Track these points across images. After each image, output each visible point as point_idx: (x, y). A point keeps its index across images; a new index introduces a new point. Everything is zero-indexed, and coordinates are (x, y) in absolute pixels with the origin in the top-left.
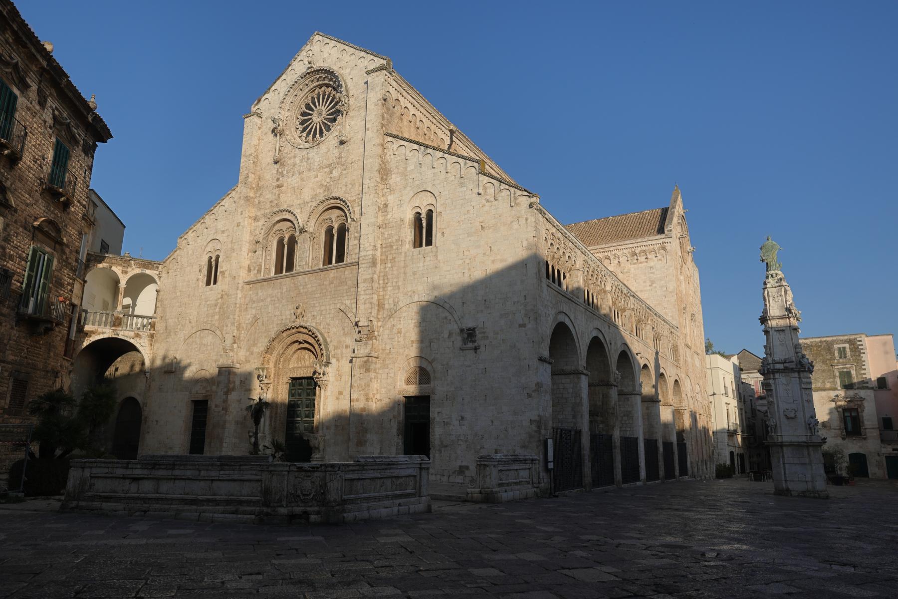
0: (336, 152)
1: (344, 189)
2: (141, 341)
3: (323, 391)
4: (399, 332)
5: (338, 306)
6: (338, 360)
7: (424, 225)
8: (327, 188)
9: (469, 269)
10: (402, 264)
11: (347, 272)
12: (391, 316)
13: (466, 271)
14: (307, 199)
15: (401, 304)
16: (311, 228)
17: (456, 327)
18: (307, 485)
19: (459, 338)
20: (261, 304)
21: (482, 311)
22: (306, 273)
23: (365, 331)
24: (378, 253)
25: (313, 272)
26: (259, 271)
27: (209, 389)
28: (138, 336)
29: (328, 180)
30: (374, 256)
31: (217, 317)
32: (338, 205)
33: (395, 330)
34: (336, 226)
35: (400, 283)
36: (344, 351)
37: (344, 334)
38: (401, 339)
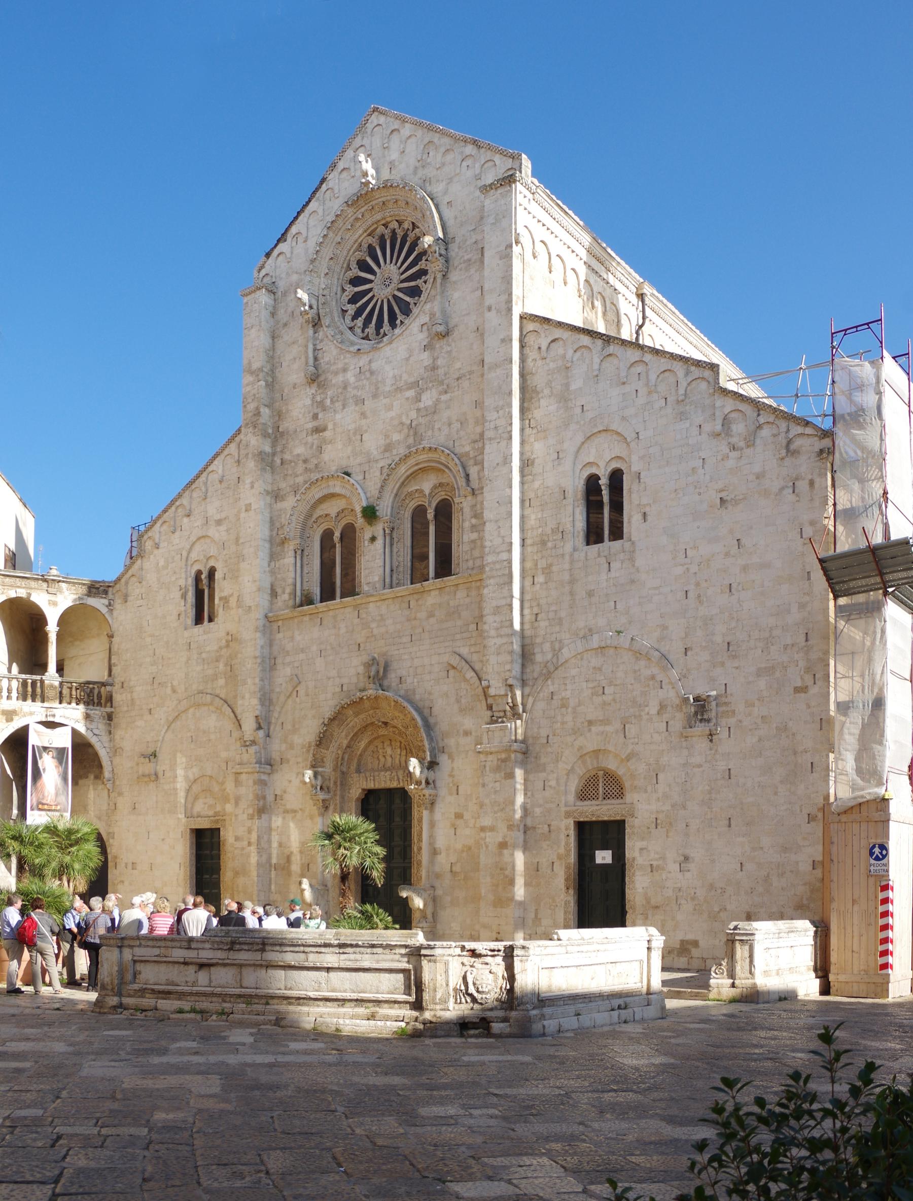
0: (426, 358)
1: (446, 430)
3: (425, 813)
4: (564, 706)
5: (446, 658)
7: (605, 493)
10: (566, 577)
11: (461, 594)
12: (548, 676)
14: (375, 453)
15: (566, 653)
17: (672, 694)
19: (679, 716)
20: (302, 656)
21: (723, 664)
27: (218, 808)
29: (413, 414)
31: (221, 682)
33: (556, 702)
35: (563, 614)
37: (462, 710)
38: (569, 718)
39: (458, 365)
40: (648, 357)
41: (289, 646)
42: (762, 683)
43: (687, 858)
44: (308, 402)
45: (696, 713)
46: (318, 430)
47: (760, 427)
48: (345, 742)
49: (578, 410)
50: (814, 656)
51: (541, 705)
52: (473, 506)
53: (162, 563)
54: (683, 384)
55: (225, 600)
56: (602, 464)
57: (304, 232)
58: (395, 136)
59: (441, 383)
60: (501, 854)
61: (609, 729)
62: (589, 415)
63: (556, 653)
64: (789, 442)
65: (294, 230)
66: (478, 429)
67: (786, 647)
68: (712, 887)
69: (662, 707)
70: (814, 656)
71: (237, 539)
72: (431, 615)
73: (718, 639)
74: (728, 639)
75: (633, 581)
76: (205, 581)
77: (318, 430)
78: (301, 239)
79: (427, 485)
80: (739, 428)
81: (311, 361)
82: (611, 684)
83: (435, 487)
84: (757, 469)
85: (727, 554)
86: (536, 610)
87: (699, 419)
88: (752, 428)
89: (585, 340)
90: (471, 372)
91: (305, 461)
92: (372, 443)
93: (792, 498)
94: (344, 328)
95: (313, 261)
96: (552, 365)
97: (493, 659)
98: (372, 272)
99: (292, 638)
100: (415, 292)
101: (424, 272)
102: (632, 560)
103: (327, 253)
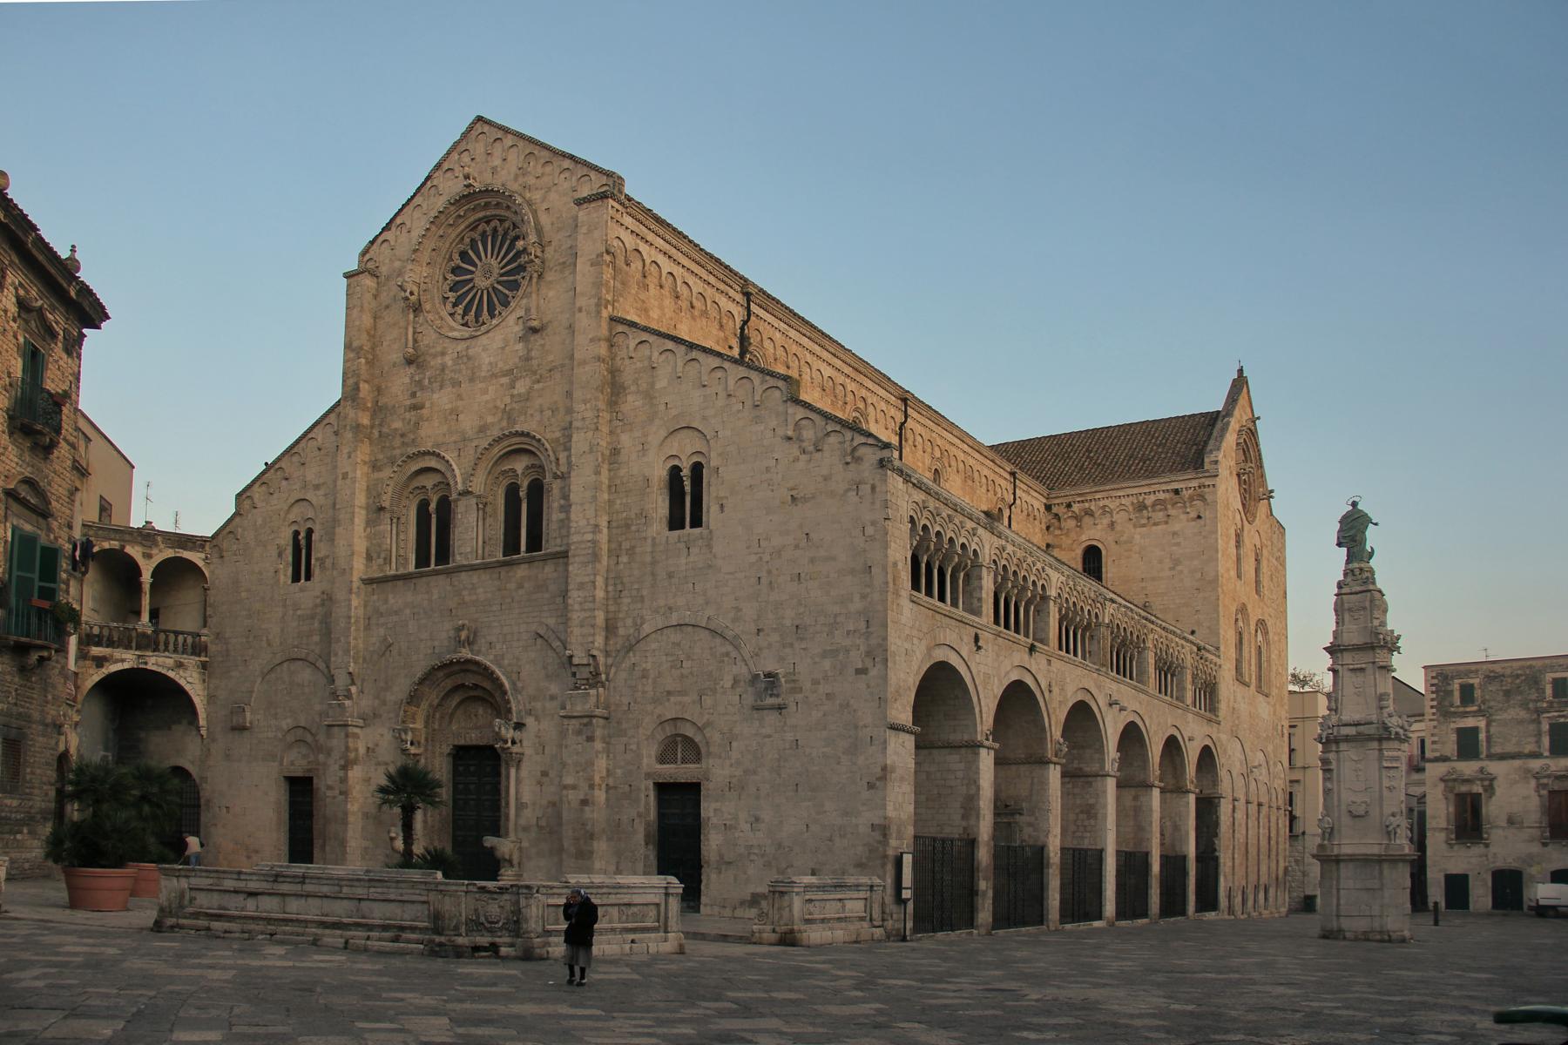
2: (188, 674)
3: (513, 771)
4: (645, 676)
5: (534, 627)
6: (537, 719)
8: (509, 415)
9: (769, 572)
10: (648, 559)
12: (630, 648)
13: (763, 574)
14: (470, 433)
15: (647, 629)
17: (744, 670)
18: (493, 909)
20: (395, 618)
21: (791, 645)
22: (472, 568)
24: (603, 537)
25: (485, 567)
26: (388, 560)
28: (180, 665)
29: (508, 400)
31: (316, 638)
34: (525, 484)
35: (645, 593)
36: (548, 705)
38: (649, 688)
39: (551, 358)
40: (727, 365)
41: (383, 609)
42: (827, 664)
43: (757, 819)
44: (407, 380)
45: (766, 689)
46: (415, 407)
47: (828, 434)
48: (436, 702)
49: (662, 407)
50: (873, 642)
51: (623, 675)
52: (562, 488)
53: (260, 522)
54: (759, 391)
55: (322, 561)
56: (684, 458)
57: (408, 224)
58: (498, 144)
59: (535, 373)
60: (582, 811)
61: (686, 699)
62: (674, 412)
63: (638, 627)
64: (854, 449)
65: (399, 221)
66: (568, 418)
67: (848, 632)
68: (780, 846)
69: (736, 682)
70: (873, 642)
71: (334, 504)
72: (520, 586)
73: (788, 622)
74: (797, 622)
75: (710, 566)
76: (303, 543)
77: (415, 407)
78: (405, 230)
79: (520, 464)
80: (808, 434)
81: (410, 343)
82: (689, 658)
83: (527, 468)
84: (825, 472)
85: (797, 547)
86: (619, 587)
87: (773, 423)
88: (820, 435)
89: (670, 345)
90: (563, 366)
91: (402, 435)
92: (468, 423)
93: (856, 499)
94: (444, 314)
95: (415, 251)
96: (639, 365)
97: (577, 631)
98: (475, 265)
99: (386, 601)
100: (514, 286)
101: (522, 268)
102: (709, 546)
103: (430, 244)
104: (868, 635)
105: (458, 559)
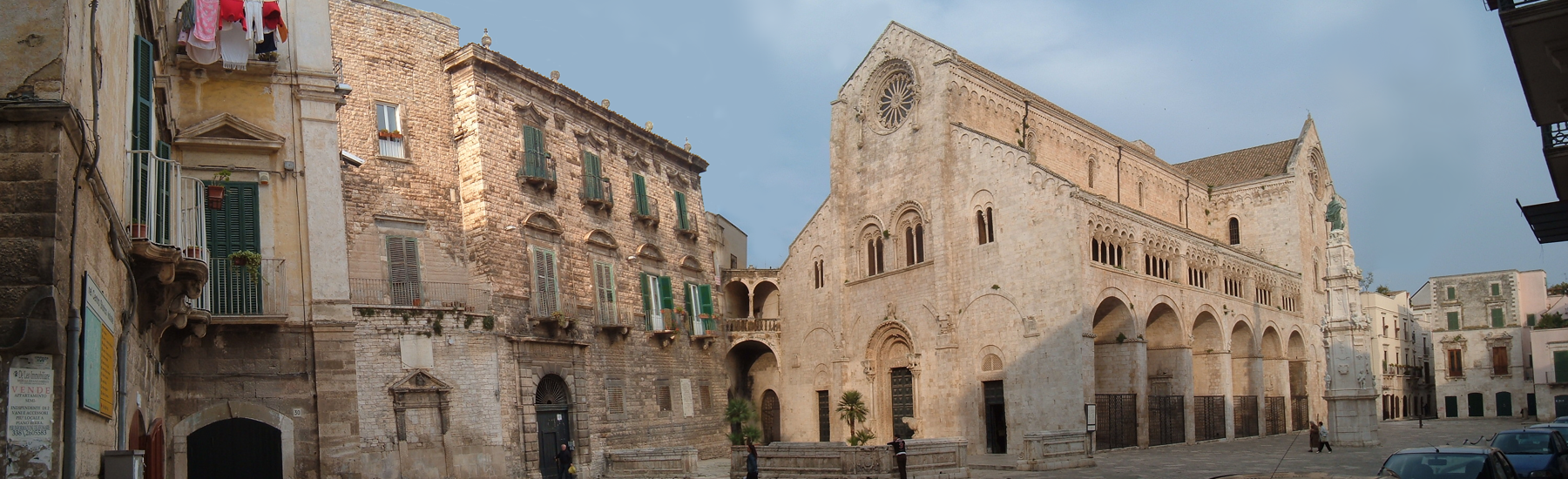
16: (892, 232)
22: (893, 273)
23: (945, 324)
25: (898, 272)
30: (946, 255)
32: (910, 208)
79: (911, 217)
92: (886, 199)
104: (1074, 292)
105: (886, 269)
